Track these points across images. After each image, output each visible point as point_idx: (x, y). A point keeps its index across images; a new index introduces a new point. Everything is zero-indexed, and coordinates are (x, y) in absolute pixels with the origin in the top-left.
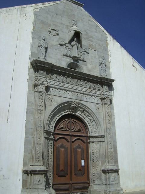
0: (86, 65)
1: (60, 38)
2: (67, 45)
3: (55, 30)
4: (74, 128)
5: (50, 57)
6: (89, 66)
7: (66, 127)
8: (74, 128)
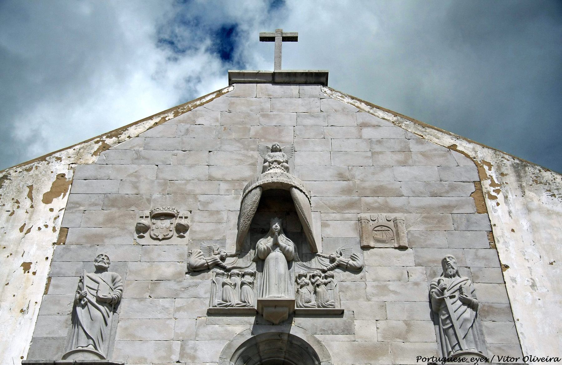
0: (348, 330)
1: (195, 241)
2: (228, 263)
3: (170, 216)
5: (132, 337)
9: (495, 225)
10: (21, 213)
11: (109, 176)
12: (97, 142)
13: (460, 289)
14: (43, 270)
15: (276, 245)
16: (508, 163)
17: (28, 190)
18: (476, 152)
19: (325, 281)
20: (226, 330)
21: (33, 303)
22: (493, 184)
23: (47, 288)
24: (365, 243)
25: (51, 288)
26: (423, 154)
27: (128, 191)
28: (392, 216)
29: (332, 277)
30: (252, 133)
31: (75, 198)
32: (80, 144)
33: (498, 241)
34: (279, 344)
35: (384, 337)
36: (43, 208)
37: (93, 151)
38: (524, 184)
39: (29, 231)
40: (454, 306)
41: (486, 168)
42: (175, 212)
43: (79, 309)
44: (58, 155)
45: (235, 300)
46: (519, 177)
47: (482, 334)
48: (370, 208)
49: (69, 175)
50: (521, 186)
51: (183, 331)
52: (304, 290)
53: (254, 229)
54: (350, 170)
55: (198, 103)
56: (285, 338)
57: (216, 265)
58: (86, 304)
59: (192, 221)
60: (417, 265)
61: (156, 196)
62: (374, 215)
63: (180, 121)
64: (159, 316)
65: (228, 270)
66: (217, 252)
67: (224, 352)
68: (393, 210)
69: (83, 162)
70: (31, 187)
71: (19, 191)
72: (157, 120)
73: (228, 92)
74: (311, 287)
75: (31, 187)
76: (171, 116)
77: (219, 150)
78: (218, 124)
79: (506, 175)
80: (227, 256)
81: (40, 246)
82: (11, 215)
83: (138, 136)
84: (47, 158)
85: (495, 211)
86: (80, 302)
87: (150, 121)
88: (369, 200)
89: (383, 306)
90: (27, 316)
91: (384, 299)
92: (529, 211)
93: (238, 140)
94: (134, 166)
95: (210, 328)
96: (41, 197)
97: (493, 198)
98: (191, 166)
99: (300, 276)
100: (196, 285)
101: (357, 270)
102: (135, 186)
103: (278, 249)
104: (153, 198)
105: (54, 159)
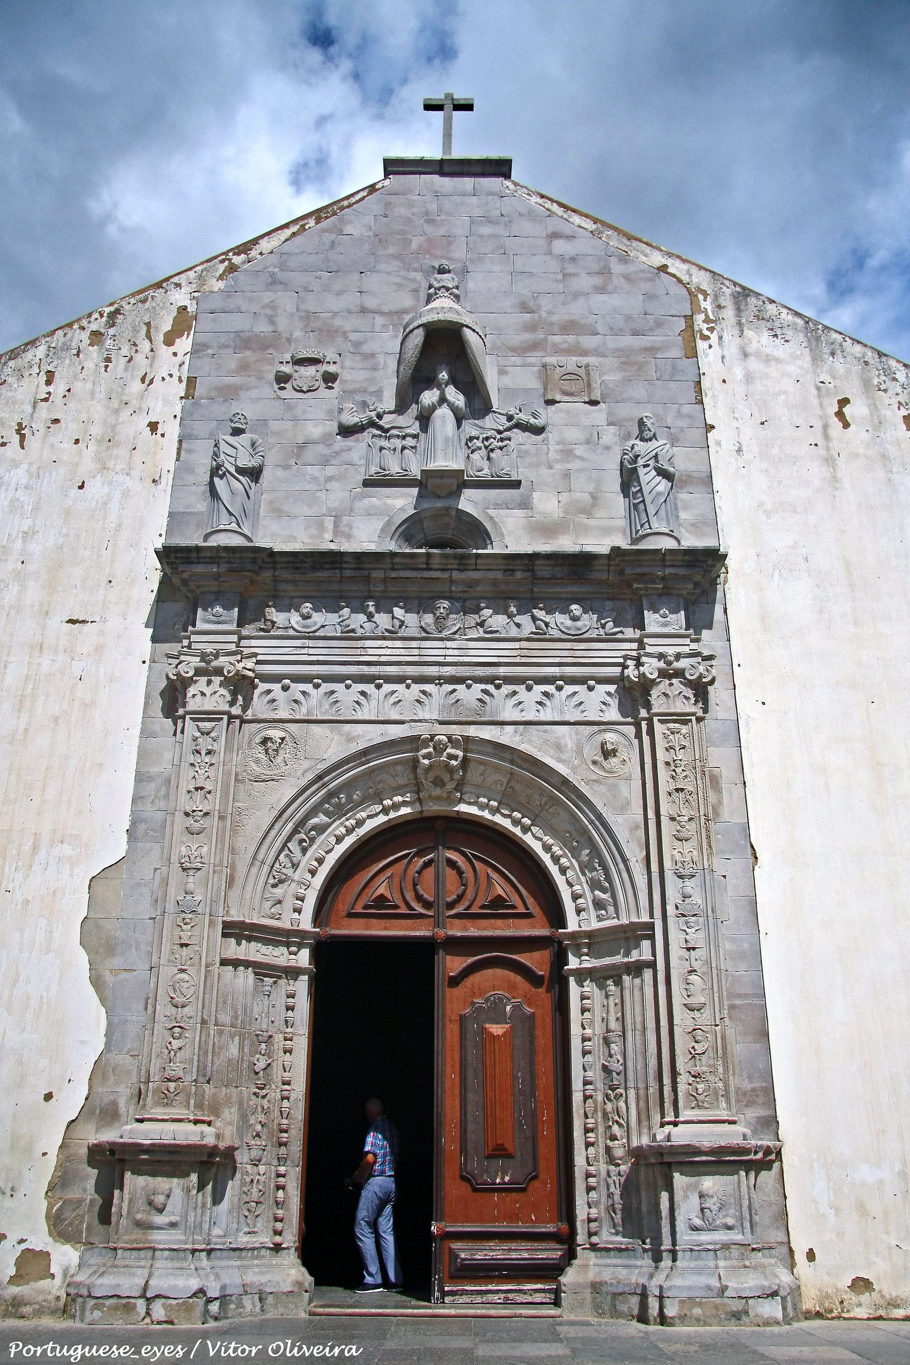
0: (525, 504)
1: (348, 394)
2: (386, 422)
4: (460, 898)
5: (278, 513)
6: (547, 504)
7: (410, 896)
8: (460, 898)
9: (704, 374)
10: (139, 358)
11: (239, 309)
12: (222, 261)
13: (656, 456)
14: (172, 430)
15: (443, 400)
16: (728, 292)
17: (145, 328)
18: (691, 275)
19: (500, 444)
20: (385, 504)
21: (164, 472)
22: (707, 320)
23: (179, 454)
24: (549, 397)
25: (183, 453)
26: (627, 278)
27: (262, 328)
28: (584, 360)
29: (509, 439)
30: (414, 246)
31: (202, 338)
32: (202, 263)
33: (706, 395)
34: (447, 519)
35: (565, 512)
36: (164, 351)
37: (218, 275)
38: (743, 321)
39: (151, 382)
40: (648, 477)
41: (701, 297)
42: (319, 356)
43: (216, 480)
44: (175, 280)
45: (395, 469)
46: (739, 310)
47: (676, 509)
48: (558, 351)
49: (192, 308)
50: (739, 324)
51: (336, 504)
52: (475, 456)
53: (416, 380)
54: (535, 299)
55: (346, 203)
56: (454, 513)
57: (372, 424)
58: (224, 474)
59: (342, 367)
60: (610, 424)
61: (298, 334)
62: (563, 359)
63: (324, 231)
64: (308, 487)
65: (386, 431)
66: (372, 408)
67: (383, 530)
68: (585, 353)
69: (208, 289)
70: (148, 325)
71: (136, 330)
72: (294, 229)
73: (383, 187)
74: (483, 452)
75: (148, 325)
76: (312, 222)
77: (373, 270)
78: (371, 234)
79: (724, 307)
80: (384, 413)
81: (167, 401)
82: (129, 361)
83: (271, 252)
84: (164, 285)
85: (706, 356)
86: (216, 471)
87: (286, 230)
88: (557, 339)
89: (567, 475)
90: (159, 487)
91: (569, 466)
92: (746, 355)
93: (397, 257)
94: (269, 293)
95: (367, 502)
96: (161, 338)
97: (705, 338)
98: (339, 293)
99: (471, 439)
100: (350, 449)
101: (538, 430)
102: (272, 322)
103: (445, 404)
104: (294, 337)
105: (173, 286)
